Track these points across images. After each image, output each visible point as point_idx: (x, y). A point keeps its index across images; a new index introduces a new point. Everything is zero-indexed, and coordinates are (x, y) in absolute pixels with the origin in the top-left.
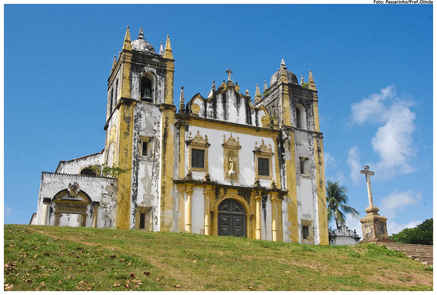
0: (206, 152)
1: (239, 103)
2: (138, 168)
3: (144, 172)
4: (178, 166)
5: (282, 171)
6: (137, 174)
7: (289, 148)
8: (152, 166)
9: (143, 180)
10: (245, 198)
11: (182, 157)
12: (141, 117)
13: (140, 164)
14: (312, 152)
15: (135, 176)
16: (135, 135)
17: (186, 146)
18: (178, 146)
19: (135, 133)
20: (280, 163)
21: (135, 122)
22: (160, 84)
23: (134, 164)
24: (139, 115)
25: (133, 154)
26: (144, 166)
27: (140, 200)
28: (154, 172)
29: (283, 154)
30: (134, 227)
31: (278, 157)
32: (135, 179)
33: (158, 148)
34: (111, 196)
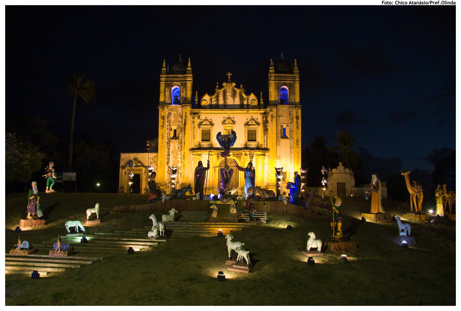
0: (211, 131)
1: (235, 94)
2: (170, 146)
3: (173, 148)
4: (193, 142)
5: (265, 136)
6: (169, 149)
7: (272, 120)
8: (178, 143)
9: (172, 152)
10: (237, 157)
11: (195, 135)
12: (171, 115)
13: (171, 143)
14: (292, 120)
15: (168, 151)
16: (168, 126)
17: (198, 128)
18: (193, 129)
19: (168, 125)
20: (264, 131)
21: (168, 118)
22: (183, 92)
23: (167, 143)
24: (170, 114)
25: (166, 138)
26: (173, 144)
27: (171, 164)
28: (179, 146)
29: (267, 125)
30: (168, 179)
31: (263, 127)
32: (168, 152)
33: (181, 132)
34: (155, 163)
